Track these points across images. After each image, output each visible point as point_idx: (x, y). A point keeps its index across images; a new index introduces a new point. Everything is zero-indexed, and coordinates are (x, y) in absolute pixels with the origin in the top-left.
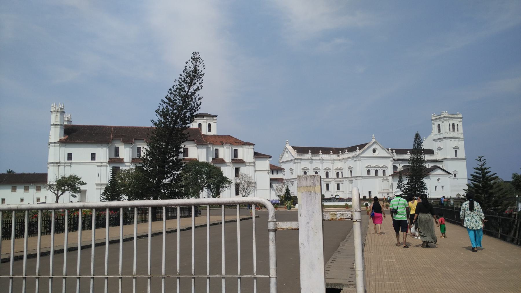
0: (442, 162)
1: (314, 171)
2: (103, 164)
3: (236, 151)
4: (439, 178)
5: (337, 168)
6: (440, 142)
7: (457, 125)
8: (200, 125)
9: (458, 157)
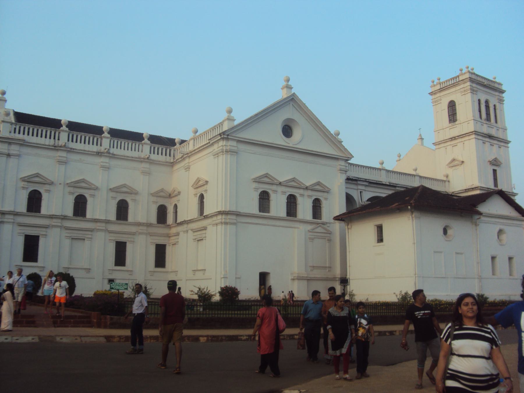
1: (71, 193)
4: (502, 227)
5: (162, 190)
7: (495, 106)
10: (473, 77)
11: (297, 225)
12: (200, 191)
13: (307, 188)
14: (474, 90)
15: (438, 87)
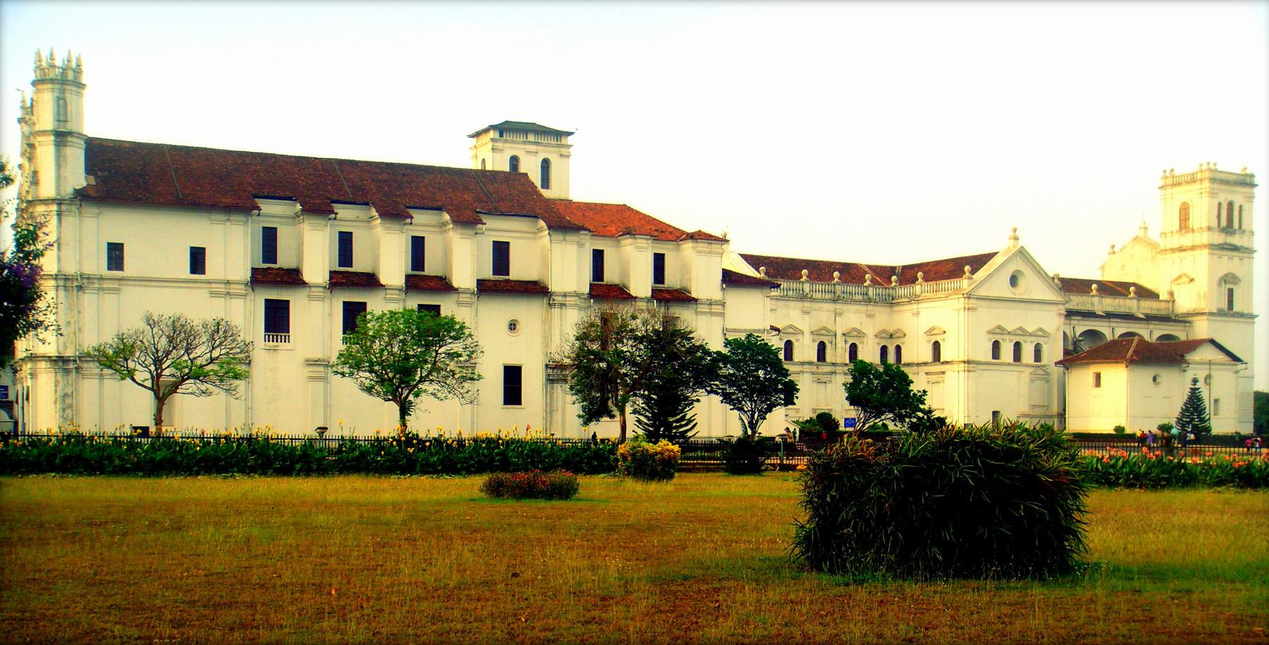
0: (1188, 324)
2: (235, 289)
3: (659, 260)
6: (1230, 258)
7: (1241, 206)
8: (514, 161)
9: (1237, 308)
10: (1215, 175)
11: (1022, 369)
12: (934, 339)
13: (1030, 335)
14: (1213, 193)
15: (1170, 181)
